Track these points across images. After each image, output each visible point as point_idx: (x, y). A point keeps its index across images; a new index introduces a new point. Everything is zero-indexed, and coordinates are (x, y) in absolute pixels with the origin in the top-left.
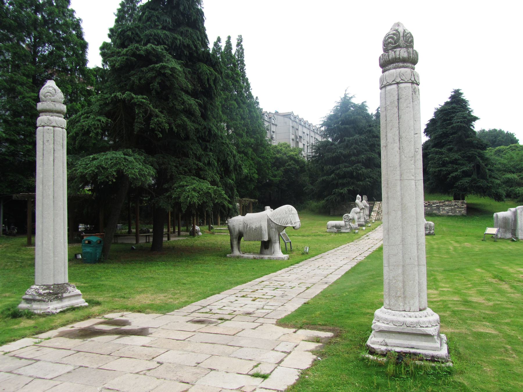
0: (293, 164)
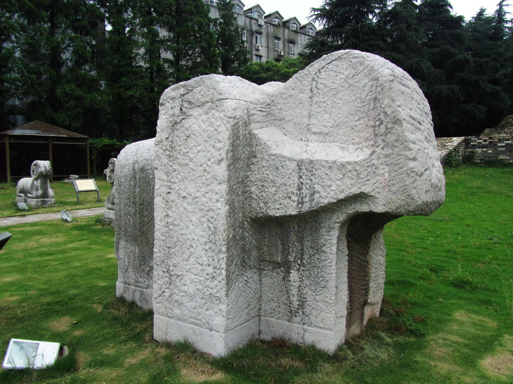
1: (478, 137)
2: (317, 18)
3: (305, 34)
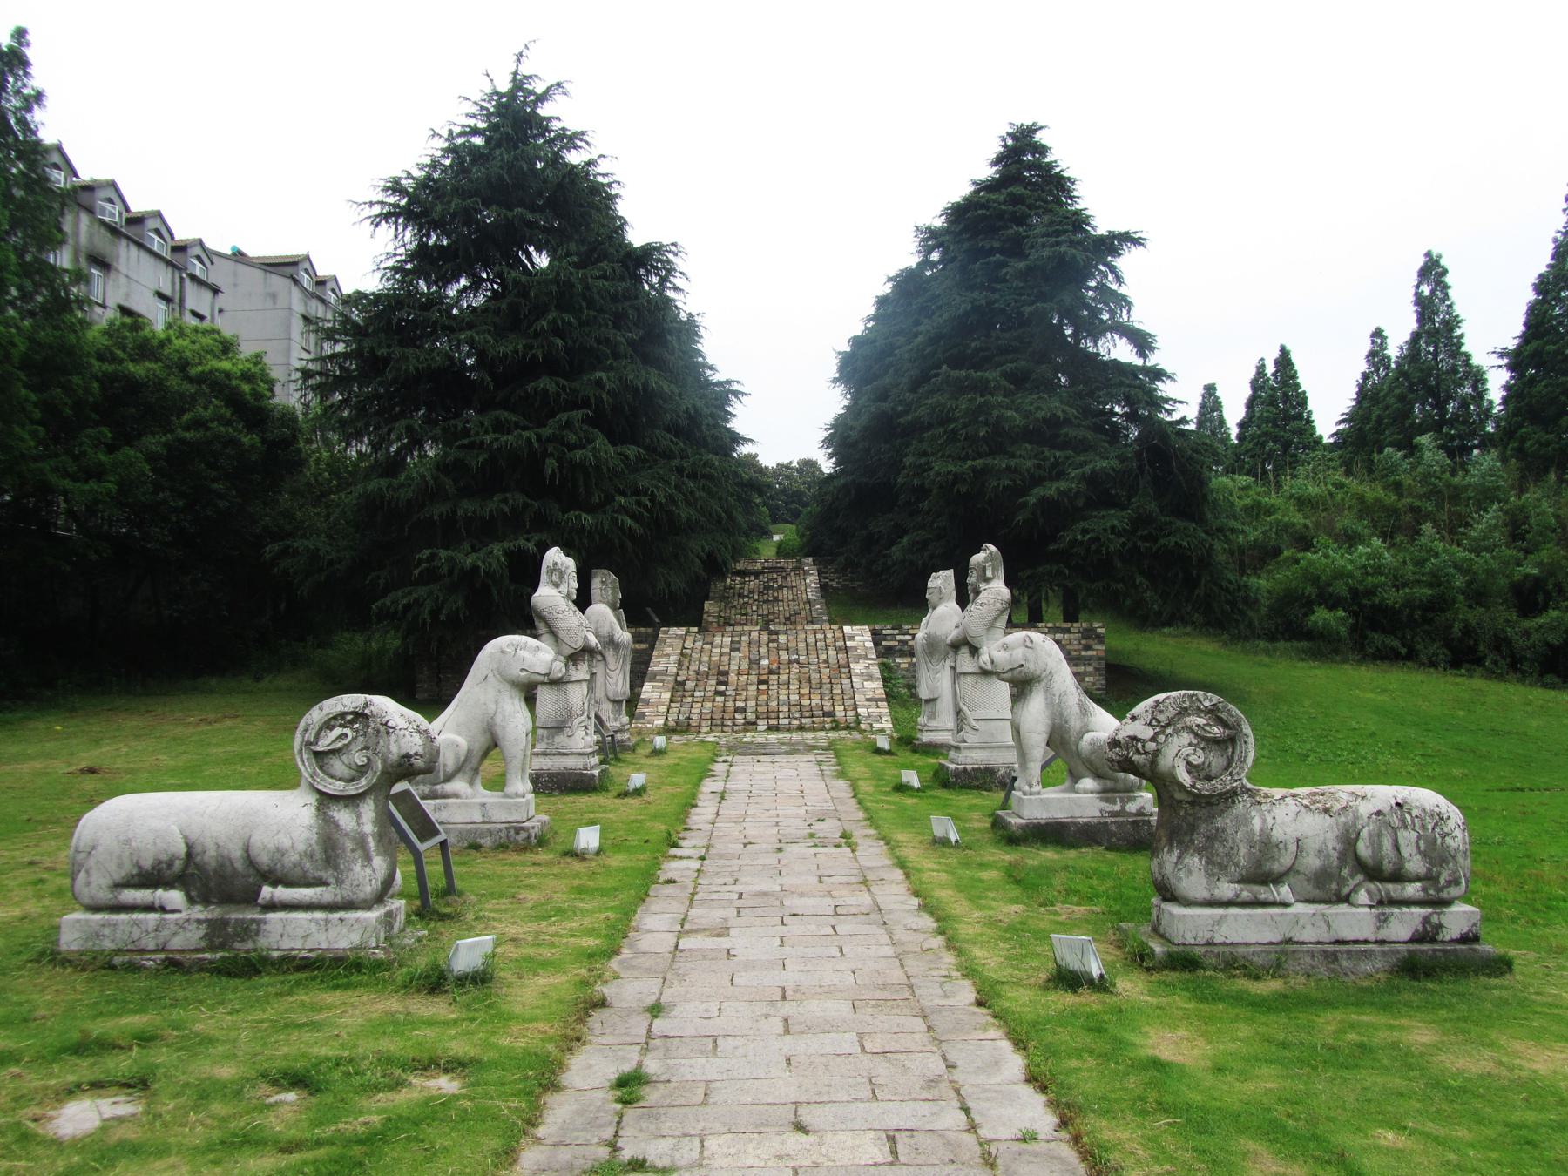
0: (219, 418)
1: (899, 627)
2: (385, 217)
3: (141, 246)
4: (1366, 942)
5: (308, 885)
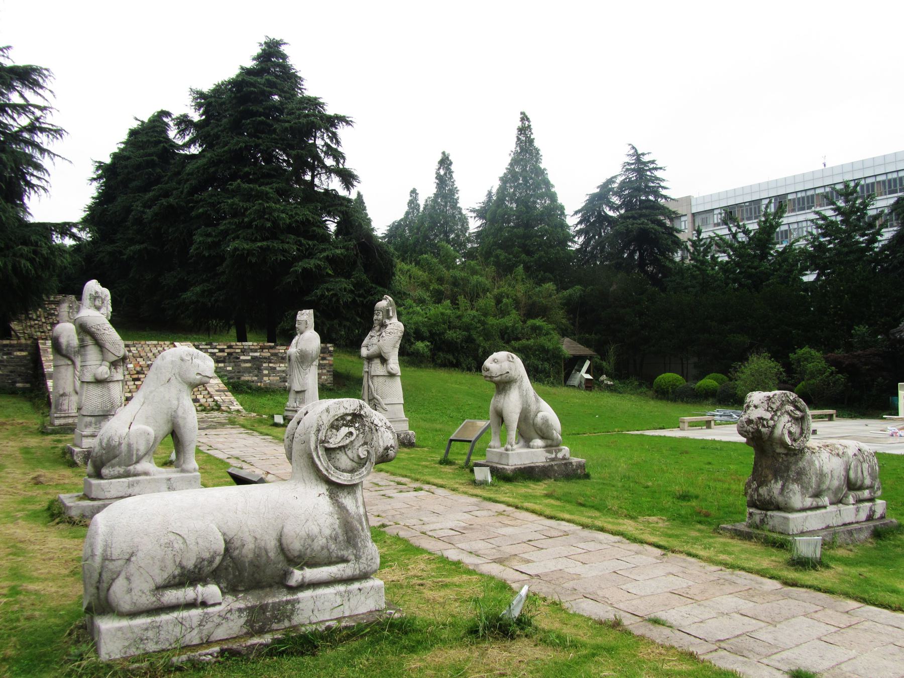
1: (210, 344)
4: (852, 523)
5: (330, 563)
